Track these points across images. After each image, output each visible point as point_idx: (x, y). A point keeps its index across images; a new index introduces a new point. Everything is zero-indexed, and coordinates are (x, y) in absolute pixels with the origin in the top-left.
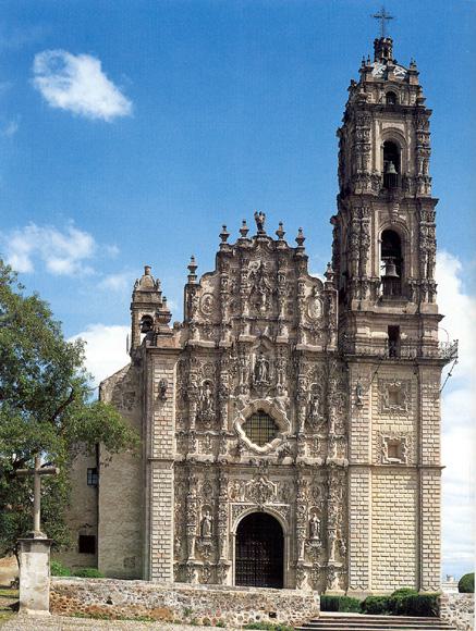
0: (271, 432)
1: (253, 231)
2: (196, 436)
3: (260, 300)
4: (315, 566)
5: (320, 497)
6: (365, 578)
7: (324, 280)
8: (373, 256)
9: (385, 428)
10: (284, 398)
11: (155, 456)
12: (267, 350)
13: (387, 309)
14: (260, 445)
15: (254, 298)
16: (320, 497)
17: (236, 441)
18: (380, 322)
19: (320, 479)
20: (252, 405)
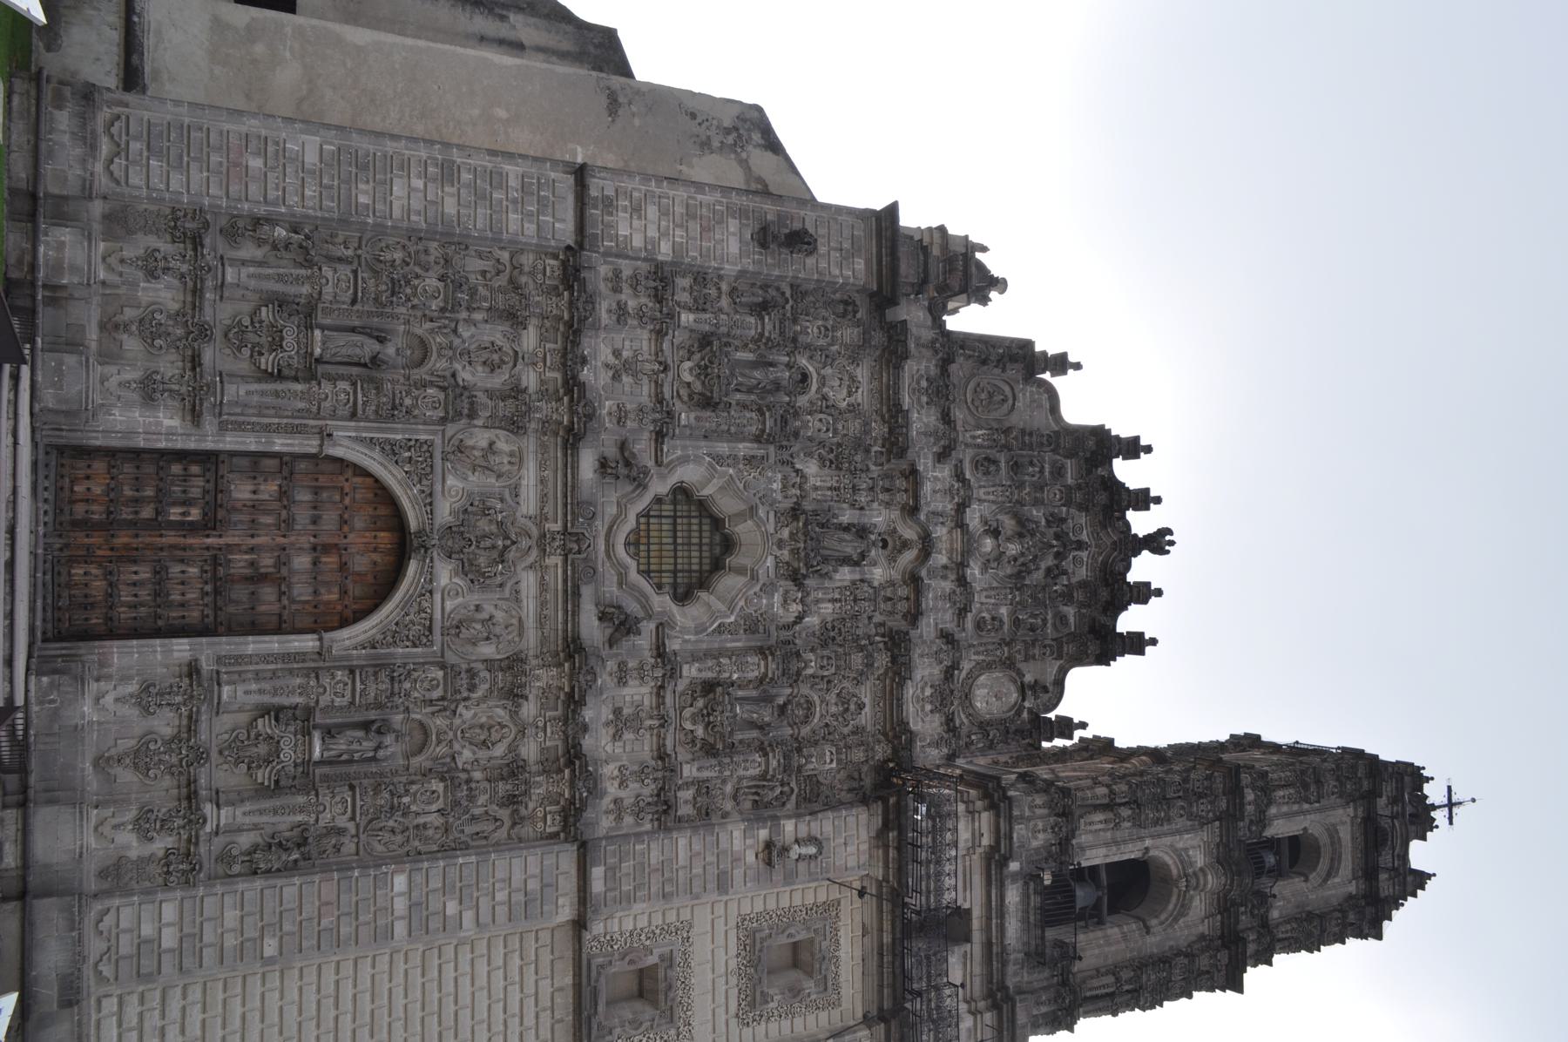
0: (667, 579)
1: (1141, 523)
2: (660, 334)
3: (1008, 539)
4: (200, 756)
5: (467, 754)
6: (148, 964)
7: (1052, 715)
8: (1116, 843)
9: (701, 949)
10: (779, 607)
11: (594, 192)
12: (892, 559)
13: (1013, 896)
14: (627, 544)
15: (1009, 524)
16: (467, 754)
17: (651, 463)
18: (978, 880)
19: (530, 751)
20: (753, 510)
